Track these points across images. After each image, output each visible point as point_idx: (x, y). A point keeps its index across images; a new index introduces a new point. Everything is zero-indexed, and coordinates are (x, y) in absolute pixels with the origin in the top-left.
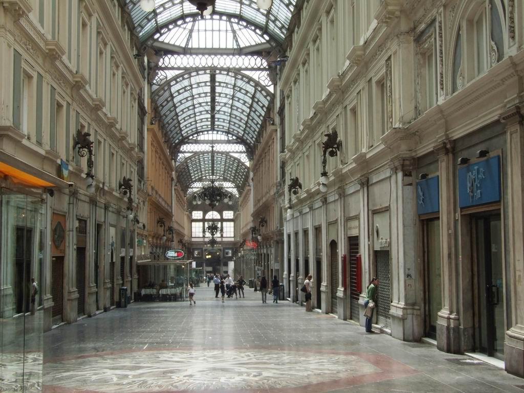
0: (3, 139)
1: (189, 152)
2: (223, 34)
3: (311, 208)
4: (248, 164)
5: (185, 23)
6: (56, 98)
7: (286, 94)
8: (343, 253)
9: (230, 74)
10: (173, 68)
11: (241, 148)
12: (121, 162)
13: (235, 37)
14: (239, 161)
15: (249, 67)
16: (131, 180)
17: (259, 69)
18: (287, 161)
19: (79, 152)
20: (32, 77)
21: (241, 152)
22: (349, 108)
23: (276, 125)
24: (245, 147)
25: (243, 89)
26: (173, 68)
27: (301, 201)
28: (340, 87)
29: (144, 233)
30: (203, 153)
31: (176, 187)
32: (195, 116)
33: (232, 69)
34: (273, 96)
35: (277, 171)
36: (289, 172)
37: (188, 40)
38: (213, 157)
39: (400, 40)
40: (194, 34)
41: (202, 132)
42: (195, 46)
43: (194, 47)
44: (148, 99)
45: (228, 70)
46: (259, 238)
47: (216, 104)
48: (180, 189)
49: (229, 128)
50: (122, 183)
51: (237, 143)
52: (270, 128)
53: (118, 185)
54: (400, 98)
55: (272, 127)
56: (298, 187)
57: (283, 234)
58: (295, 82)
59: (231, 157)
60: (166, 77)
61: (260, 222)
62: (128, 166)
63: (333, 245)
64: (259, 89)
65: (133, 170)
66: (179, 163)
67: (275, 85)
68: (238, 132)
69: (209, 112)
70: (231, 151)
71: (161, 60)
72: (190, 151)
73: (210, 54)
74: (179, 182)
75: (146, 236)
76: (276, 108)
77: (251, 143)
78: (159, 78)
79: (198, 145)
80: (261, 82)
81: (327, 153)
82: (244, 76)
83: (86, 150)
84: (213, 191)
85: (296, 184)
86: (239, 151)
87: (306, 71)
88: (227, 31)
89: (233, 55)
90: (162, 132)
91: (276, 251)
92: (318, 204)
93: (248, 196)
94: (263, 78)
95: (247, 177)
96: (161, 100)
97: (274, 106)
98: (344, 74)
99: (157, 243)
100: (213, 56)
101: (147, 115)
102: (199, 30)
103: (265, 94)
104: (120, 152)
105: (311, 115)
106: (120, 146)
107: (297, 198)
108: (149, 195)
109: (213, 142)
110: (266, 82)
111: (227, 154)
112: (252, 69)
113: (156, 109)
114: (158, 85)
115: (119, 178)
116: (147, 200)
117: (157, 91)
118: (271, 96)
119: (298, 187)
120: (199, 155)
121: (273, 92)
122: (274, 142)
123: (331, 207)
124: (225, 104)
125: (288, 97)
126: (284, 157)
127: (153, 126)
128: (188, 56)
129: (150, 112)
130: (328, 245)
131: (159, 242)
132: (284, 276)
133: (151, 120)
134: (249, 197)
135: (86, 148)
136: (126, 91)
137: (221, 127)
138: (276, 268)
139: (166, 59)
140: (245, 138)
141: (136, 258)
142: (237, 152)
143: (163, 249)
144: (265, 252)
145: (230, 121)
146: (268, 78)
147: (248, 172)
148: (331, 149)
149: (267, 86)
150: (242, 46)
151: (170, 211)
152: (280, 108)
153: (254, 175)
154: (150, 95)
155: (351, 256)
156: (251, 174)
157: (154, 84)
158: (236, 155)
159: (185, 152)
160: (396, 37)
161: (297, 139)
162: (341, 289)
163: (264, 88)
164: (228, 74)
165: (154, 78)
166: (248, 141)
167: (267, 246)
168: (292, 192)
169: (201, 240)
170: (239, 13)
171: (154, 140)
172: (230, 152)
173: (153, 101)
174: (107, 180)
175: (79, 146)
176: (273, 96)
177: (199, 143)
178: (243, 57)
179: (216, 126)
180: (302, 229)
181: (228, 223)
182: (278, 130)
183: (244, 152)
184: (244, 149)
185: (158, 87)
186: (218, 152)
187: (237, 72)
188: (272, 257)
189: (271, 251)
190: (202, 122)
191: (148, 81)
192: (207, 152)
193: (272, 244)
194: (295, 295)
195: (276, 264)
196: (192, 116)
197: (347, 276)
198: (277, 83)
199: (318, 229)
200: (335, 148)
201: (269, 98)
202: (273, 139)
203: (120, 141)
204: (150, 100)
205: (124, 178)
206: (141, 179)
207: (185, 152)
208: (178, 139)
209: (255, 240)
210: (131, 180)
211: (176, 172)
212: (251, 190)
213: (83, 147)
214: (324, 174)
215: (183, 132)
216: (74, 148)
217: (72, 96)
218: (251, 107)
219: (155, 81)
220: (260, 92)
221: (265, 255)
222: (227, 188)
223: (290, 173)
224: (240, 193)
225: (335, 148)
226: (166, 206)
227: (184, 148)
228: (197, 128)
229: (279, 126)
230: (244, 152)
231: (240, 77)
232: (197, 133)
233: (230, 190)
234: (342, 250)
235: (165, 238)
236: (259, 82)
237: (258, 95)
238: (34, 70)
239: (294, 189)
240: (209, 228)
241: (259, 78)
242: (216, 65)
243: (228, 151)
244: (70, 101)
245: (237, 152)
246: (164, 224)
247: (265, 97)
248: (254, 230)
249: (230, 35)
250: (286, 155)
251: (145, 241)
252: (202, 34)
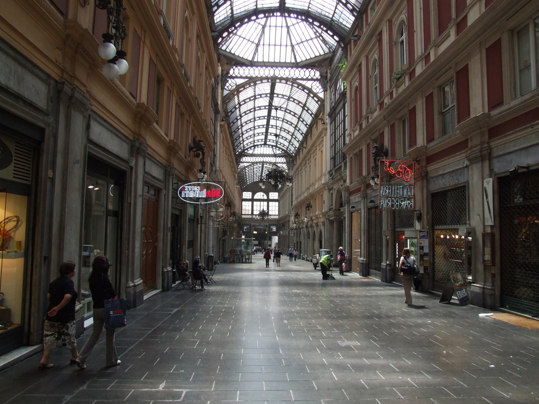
1: (247, 162)
2: (283, 48)
5: (257, 18)
9: (288, 83)
10: (241, 77)
11: (283, 160)
13: (293, 50)
15: (305, 77)
17: (312, 79)
21: (282, 163)
26: (241, 77)
30: (257, 163)
33: (290, 79)
37: (255, 54)
40: (260, 48)
41: (257, 145)
42: (260, 60)
43: (259, 61)
45: (287, 80)
55: (324, 126)
60: (236, 84)
61: (307, 207)
64: (312, 95)
71: (232, 70)
73: (272, 67)
82: (299, 85)
86: (281, 162)
88: (286, 45)
89: (292, 67)
94: (315, 87)
96: (230, 106)
100: (274, 68)
102: (264, 45)
103: (317, 100)
112: (307, 79)
113: (227, 114)
114: (229, 90)
117: (227, 96)
128: (254, 68)
139: (236, 70)
150: (299, 60)
163: (315, 95)
164: (286, 83)
165: (225, 85)
170: (307, 8)
178: (300, 69)
179: (268, 140)
183: (285, 163)
185: (228, 92)
187: (293, 82)
191: (221, 86)
196: (252, 129)
208: (241, 149)
211: (238, 176)
215: (245, 143)
220: (313, 98)
227: (244, 159)
230: (285, 163)
231: (296, 85)
232: (254, 146)
236: (311, 89)
241: (312, 87)
242: (277, 76)
245: (280, 163)
249: (289, 49)
252: (266, 47)
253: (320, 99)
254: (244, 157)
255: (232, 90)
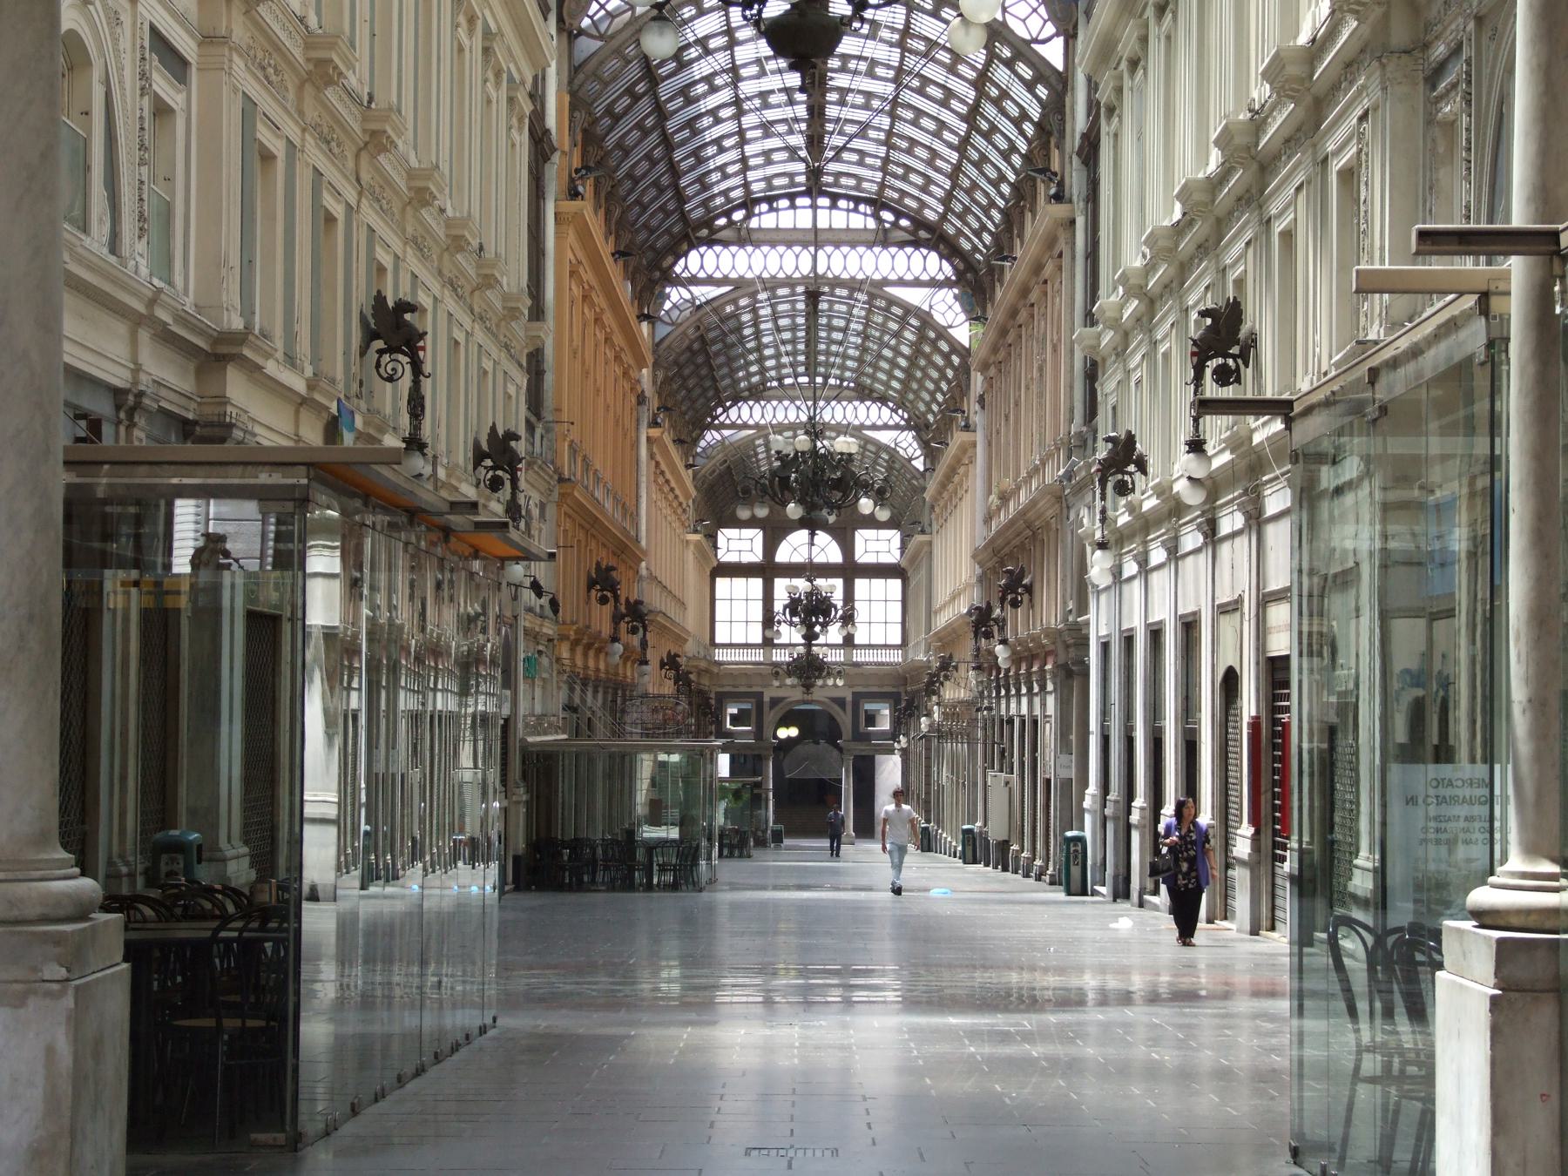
0: (225, 368)
1: (710, 281)
3: (1143, 561)
4: (963, 333)
6: (325, 203)
7: (1104, 96)
8: (1253, 713)
11: (933, 264)
12: (480, 367)
14: (926, 319)
16: (517, 438)
18: (1104, 360)
19: (378, 365)
20: (274, 157)
21: (933, 284)
22: (1278, 227)
23: (1070, 201)
24: (954, 267)
25: (944, 48)
27: (1144, 525)
28: (1253, 151)
29: (545, 630)
30: (771, 285)
31: (655, 432)
32: (743, 142)
34: (1059, 83)
35: (1071, 388)
36: (1112, 400)
38: (813, 297)
39: (1388, 75)
44: (558, 91)
46: (999, 649)
47: (829, 127)
48: (667, 439)
49: (882, 186)
50: (485, 446)
51: (917, 244)
52: (1047, 214)
53: (470, 455)
54: (1382, 248)
55: (1059, 210)
56: (1132, 468)
57: (1084, 643)
58: (1134, 64)
59: (892, 301)
61: (1006, 590)
62: (500, 376)
63: (1230, 682)
64: (1007, 53)
65: (512, 390)
66: (669, 329)
67: (1070, 36)
68: (923, 205)
69: (803, 153)
70: (893, 277)
72: (718, 275)
74: (667, 409)
75: (550, 640)
76: (1073, 130)
77: (975, 249)
78: (602, 7)
79: (750, 249)
80: (1013, 24)
81: (1208, 372)
83: (401, 357)
84: (818, 470)
85: (1125, 455)
86: (925, 277)
87: (1168, 38)
90: (608, 213)
91: (1064, 705)
92: (1191, 539)
93: (962, 470)
95: (961, 388)
97: (1063, 120)
98: (1318, 46)
99: (586, 667)
101: (556, 158)
103: (1026, 72)
104: (480, 336)
105: (1177, 215)
106: (477, 309)
107: (1131, 508)
108: (561, 480)
109: (815, 239)
110: (1035, 23)
111: (875, 289)
114: (601, 37)
115: (475, 428)
116: (555, 496)
117: (594, 61)
118: (1053, 80)
119: (1132, 468)
120: (753, 295)
121: (1060, 66)
122: (1060, 268)
123: (1225, 549)
124: (864, 128)
125: (1111, 110)
126: (1093, 342)
127: (577, 203)
129: (567, 148)
130: (1217, 685)
131: (591, 663)
132: (1087, 804)
133: (572, 180)
134: (966, 475)
135: (405, 354)
136: (494, 94)
137: (852, 182)
138: (1064, 774)
140: (951, 231)
141: (520, 725)
142: (917, 283)
143: (605, 693)
144: (1024, 711)
145: (886, 160)
146: (1042, 10)
147: (964, 371)
148: (1220, 361)
149: (1036, 41)
151: (633, 533)
152: (1084, 136)
153: (989, 381)
154: (566, 74)
155: (1275, 722)
156: (977, 382)
157: (581, 32)
158: (914, 296)
159: (694, 281)
160: (1375, 64)
161: (1135, 289)
162: (1246, 830)
163: (1023, 51)
166: (966, 246)
167: (1030, 689)
168: (1110, 486)
169: (758, 656)
171: (581, 255)
172: (886, 282)
173: (577, 101)
174: (442, 447)
175: (379, 344)
176: (1059, 83)
177: (757, 244)
180: (1147, 626)
181: (878, 583)
182: (1080, 222)
184: (948, 269)
186: (837, 282)
188: (1049, 733)
189: (1044, 705)
190: (769, 162)
192: (790, 282)
193: (1050, 687)
194: (1122, 870)
195: (1064, 758)
197: (1263, 789)
198: (1075, 27)
199: (1189, 626)
200: (1234, 357)
201: (1042, 91)
202: (1060, 255)
203: (477, 293)
204: (567, 98)
205: (493, 428)
206: (533, 419)
207: (694, 281)
209: (984, 664)
210: (517, 438)
212: (974, 445)
213: (391, 349)
214: (1196, 446)
216: (363, 351)
217: (358, 180)
218: (972, 115)
219: (586, 22)
220: (1009, 64)
221: (1023, 722)
222: (874, 427)
223: (1114, 408)
224: (931, 455)
225: (1234, 357)
226: (618, 516)
227: (695, 262)
228: (746, 185)
229: (1082, 204)
230: (947, 283)
233: (885, 437)
234: (1249, 704)
235: (619, 647)
236: (1004, 24)
237: (1001, 74)
238: (278, 137)
239: (1119, 477)
240: (793, 606)
241: (1004, 10)
243: (877, 277)
244: (351, 195)
246: (614, 591)
247: (1030, 86)
248: (982, 622)
250: (1100, 335)
251: (545, 661)
253: (1048, 73)
254: (692, 246)
255: (612, 37)
